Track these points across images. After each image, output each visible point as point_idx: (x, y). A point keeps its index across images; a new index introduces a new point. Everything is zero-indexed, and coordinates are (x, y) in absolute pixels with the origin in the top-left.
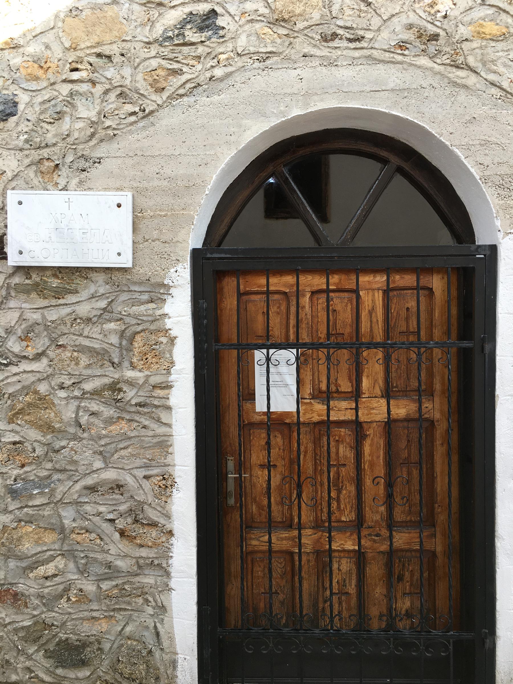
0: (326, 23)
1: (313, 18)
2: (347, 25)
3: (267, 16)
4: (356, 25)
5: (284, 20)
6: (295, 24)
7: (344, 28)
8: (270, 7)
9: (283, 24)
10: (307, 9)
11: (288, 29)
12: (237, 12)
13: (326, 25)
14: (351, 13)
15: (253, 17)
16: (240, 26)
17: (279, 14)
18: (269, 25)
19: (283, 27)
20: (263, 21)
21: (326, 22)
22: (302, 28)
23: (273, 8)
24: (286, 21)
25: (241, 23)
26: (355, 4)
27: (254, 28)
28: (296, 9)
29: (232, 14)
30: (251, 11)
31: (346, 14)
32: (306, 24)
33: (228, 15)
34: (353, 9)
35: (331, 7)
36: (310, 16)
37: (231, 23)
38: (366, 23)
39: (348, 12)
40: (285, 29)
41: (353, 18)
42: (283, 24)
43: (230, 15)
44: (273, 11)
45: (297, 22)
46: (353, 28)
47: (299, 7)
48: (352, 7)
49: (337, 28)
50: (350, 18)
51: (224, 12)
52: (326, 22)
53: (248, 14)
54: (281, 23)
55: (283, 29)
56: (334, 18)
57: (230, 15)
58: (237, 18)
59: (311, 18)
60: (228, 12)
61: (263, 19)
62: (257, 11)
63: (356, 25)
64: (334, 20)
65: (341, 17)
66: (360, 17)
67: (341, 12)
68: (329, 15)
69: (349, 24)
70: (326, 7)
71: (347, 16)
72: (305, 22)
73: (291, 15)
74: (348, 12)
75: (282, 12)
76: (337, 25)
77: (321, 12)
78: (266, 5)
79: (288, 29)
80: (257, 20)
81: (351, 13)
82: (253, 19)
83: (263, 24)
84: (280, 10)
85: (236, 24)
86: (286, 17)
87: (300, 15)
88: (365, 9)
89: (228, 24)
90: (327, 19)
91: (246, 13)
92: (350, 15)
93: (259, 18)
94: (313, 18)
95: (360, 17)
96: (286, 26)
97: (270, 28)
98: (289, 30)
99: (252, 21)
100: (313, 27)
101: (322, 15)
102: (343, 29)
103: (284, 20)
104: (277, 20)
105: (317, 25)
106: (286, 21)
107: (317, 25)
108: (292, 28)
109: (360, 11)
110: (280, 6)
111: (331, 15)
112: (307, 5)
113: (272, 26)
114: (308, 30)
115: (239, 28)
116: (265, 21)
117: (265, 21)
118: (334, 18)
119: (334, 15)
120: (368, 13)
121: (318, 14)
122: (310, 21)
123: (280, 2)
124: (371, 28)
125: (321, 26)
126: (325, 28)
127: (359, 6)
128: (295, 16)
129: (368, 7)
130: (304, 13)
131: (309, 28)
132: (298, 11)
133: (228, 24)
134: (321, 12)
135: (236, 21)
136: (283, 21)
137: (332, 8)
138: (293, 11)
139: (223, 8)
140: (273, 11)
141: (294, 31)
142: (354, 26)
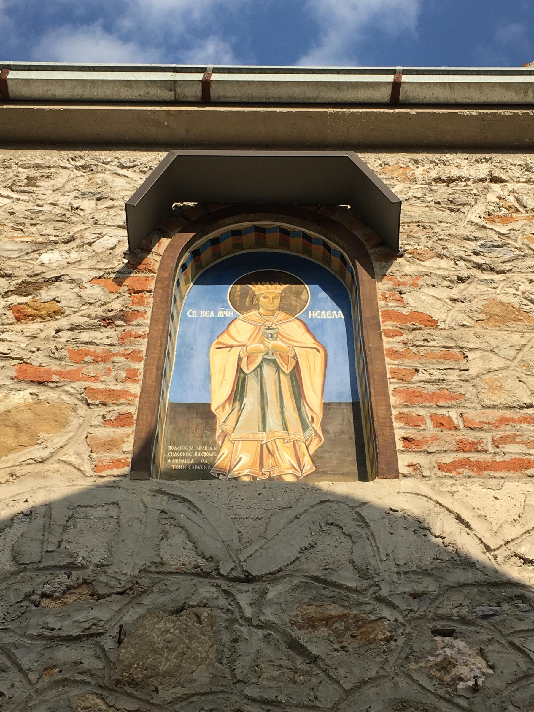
0: (222, 692)
1: (195, 681)
2: (266, 696)
3: (99, 674)
4: (286, 698)
5: (133, 683)
6: (157, 691)
7: (259, 701)
8: (107, 657)
9: (129, 691)
10: (184, 665)
11: (140, 699)
12: (36, 664)
13: (221, 695)
14: (275, 674)
15: (67, 676)
16: (36, 692)
17: (123, 671)
18: (100, 692)
19: (130, 695)
20: (89, 683)
21: (222, 688)
22: (169, 699)
23: (113, 659)
24: (137, 684)
25: (39, 685)
26: (284, 658)
27: (65, 696)
28: (160, 662)
29: (25, 667)
30: (65, 664)
31: (265, 675)
32: (179, 691)
33: (15, 670)
34: (281, 666)
35: (234, 661)
36: (189, 677)
37: (17, 684)
38: (308, 695)
39: (270, 672)
40: (134, 700)
41: (280, 684)
42: (129, 691)
43: (21, 670)
44: (111, 665)
45: (160, 688)
46: (280, 702)
47: (167, 660)
48: (278, 663)
49: (245, 701)
50: (273, 684)
51: (9, 664)
52: (222, 688)
53: (58, 670)
54: (126, 688)
55: (130, 699)
56: (239, 681)
57: (21, 670)
58: (33, 677)
59: (192, 681)
60: (18, 665)
61: (88, 679)
62: (78, 663)
63: (286, 698)
64: (238, 685)
65: (254, 680)
66: (295, 683)
67: (255, 671)
68: (229, 677)
69: (271, 695)
70: (225, 662)
71: (268, 679)
72: (178, 689)
73: (149, 673)
74: (270, 672)
75: (131, 666)
76: (246, 696)
77: (212, 671)
78: (99, 653)
79: (140, 699)
80: (75, 681)
81: (275, 674)
82: (66, 679)
83: (88, 688)
84: (126, 663)
85: (29, 687)
86: (138, 676)
87: (169, 674)
88: (306, 668)
89: (13, 686)
90: (224, 683)
91: (55, 667)
92: (274, 679)
93: (80, 678)
94: (195, 681)
95: (295, 683)
96: (136, 693)
97: (101, 697)
98: (141, 703)
99: (64, 682)
100: (195, 699)
101: (214, 676)
102: (257, 705)
103: (133, 683)
104: (118, 682)
105: (203, 694)
106: (137, 684)
107: (203, 694)
108: (148, 698)
109: (295, 671)
110: (126, 656)
111: (234, 676)
112: (185, 657)
113: (105, 693)
114: (182, 704)
115: (34, 696)
116: (93, 683)
117: (93, 683)
118: (239, 681)
119: (239, 677)
120: (311, 675)
121: (207, 674)
122: (188, 686)
123: (130, 649)
124: (318, 704)
125: (211, 697)
126: (219, 701)
127: (293, 661)
128: (158, 675)
129: (311, 665)
130: (177, 671)
131: (185, 699)
132: (163, 667)
133: (13, 686)
134: (212, 671)
135: (30, 682)
136: (130, 684)
137: (236, 663)
138: (156, 667)
139: (9, 657)
140: (111, 665)
141: (153, 704)
142: (283, 698)
